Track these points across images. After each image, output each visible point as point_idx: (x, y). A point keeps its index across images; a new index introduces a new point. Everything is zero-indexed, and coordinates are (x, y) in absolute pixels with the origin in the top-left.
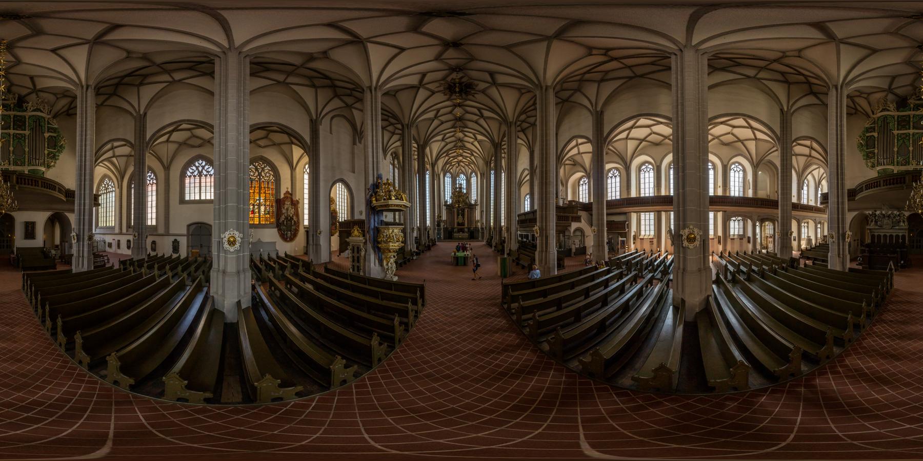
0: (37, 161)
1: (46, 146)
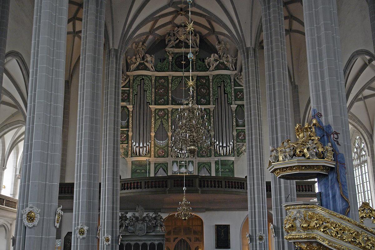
0: (225, 149)
1: (235, 124)
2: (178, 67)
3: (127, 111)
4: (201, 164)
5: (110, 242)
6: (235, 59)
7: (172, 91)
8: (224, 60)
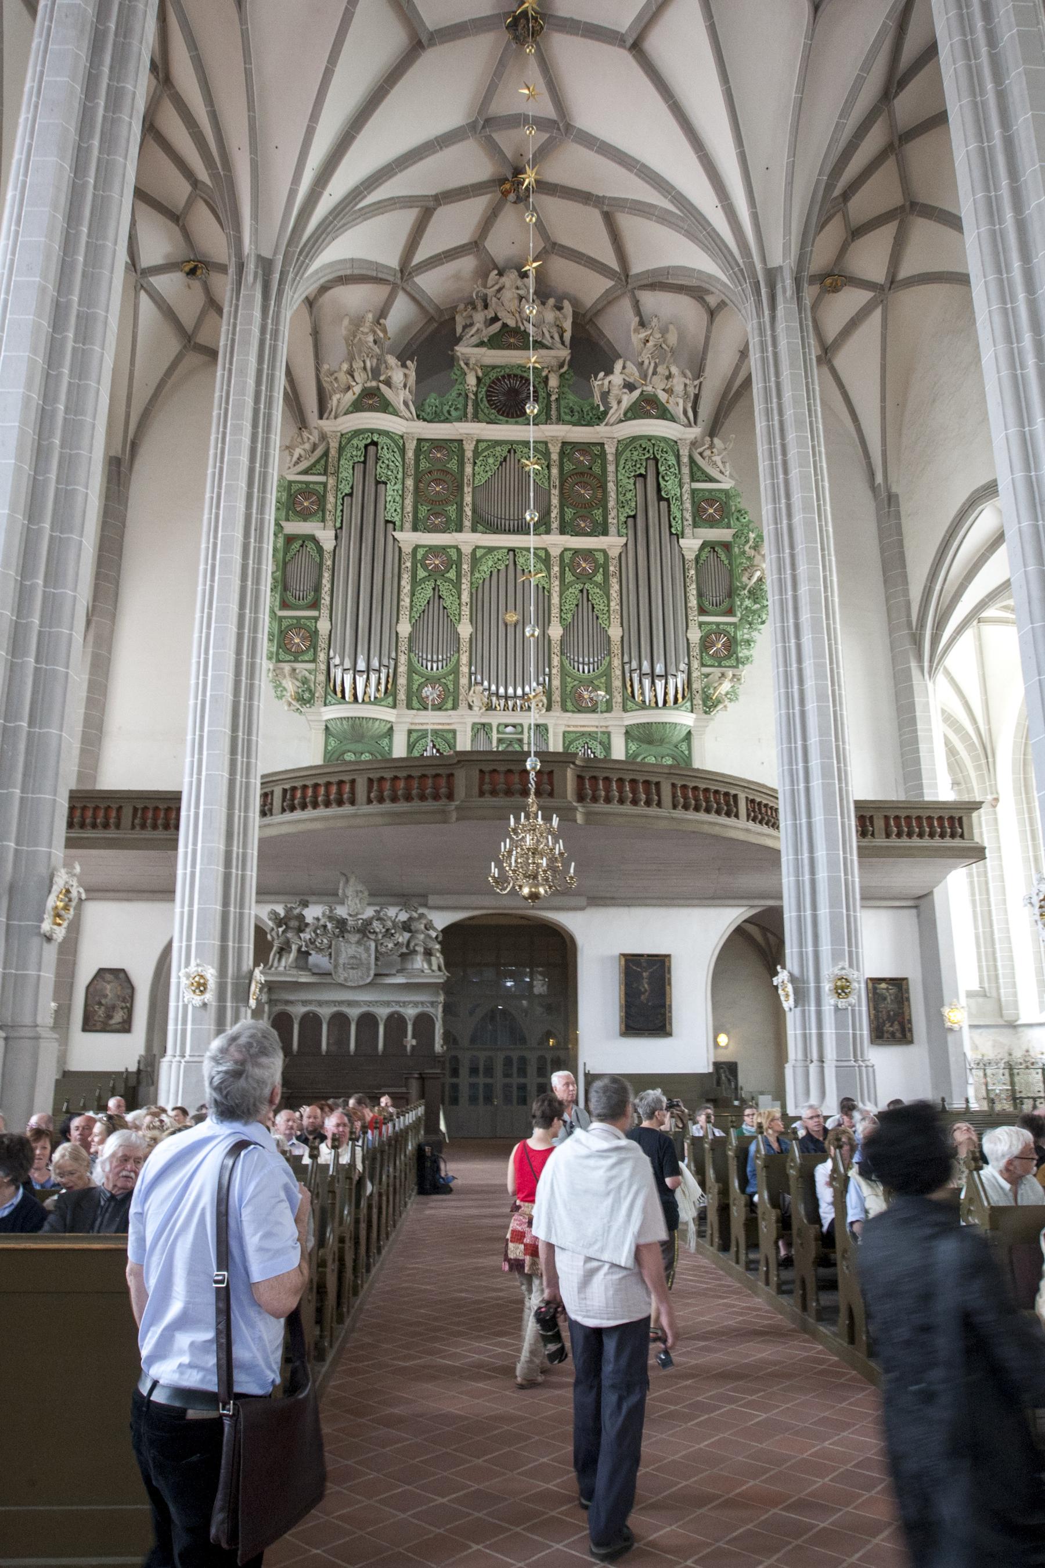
0: (660, 684)
1: (693, 602)
2: (498, 412)
3: (314, 554)
4: (572, 736)
5: (209, 996)
6: (697, 382)
7: (474, 488)
8: (656, 387)
